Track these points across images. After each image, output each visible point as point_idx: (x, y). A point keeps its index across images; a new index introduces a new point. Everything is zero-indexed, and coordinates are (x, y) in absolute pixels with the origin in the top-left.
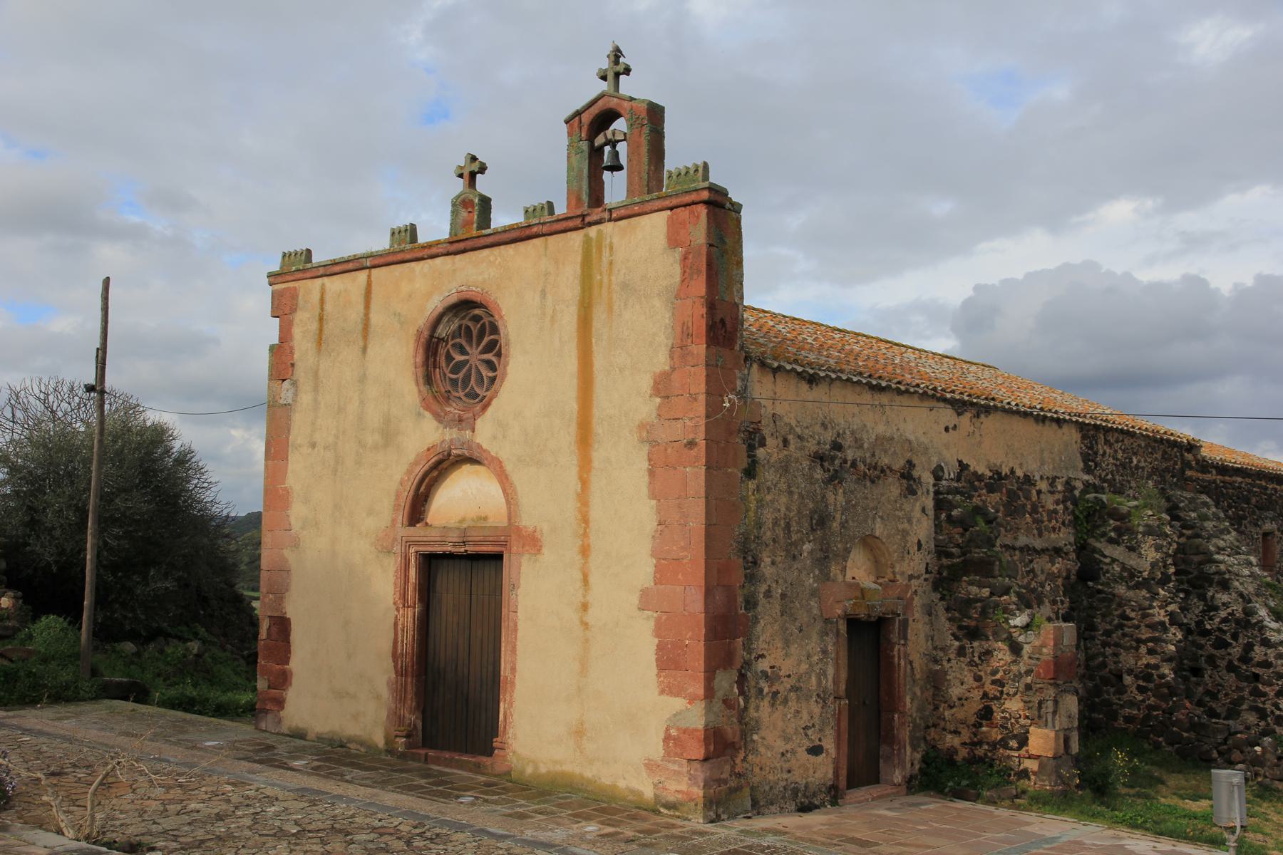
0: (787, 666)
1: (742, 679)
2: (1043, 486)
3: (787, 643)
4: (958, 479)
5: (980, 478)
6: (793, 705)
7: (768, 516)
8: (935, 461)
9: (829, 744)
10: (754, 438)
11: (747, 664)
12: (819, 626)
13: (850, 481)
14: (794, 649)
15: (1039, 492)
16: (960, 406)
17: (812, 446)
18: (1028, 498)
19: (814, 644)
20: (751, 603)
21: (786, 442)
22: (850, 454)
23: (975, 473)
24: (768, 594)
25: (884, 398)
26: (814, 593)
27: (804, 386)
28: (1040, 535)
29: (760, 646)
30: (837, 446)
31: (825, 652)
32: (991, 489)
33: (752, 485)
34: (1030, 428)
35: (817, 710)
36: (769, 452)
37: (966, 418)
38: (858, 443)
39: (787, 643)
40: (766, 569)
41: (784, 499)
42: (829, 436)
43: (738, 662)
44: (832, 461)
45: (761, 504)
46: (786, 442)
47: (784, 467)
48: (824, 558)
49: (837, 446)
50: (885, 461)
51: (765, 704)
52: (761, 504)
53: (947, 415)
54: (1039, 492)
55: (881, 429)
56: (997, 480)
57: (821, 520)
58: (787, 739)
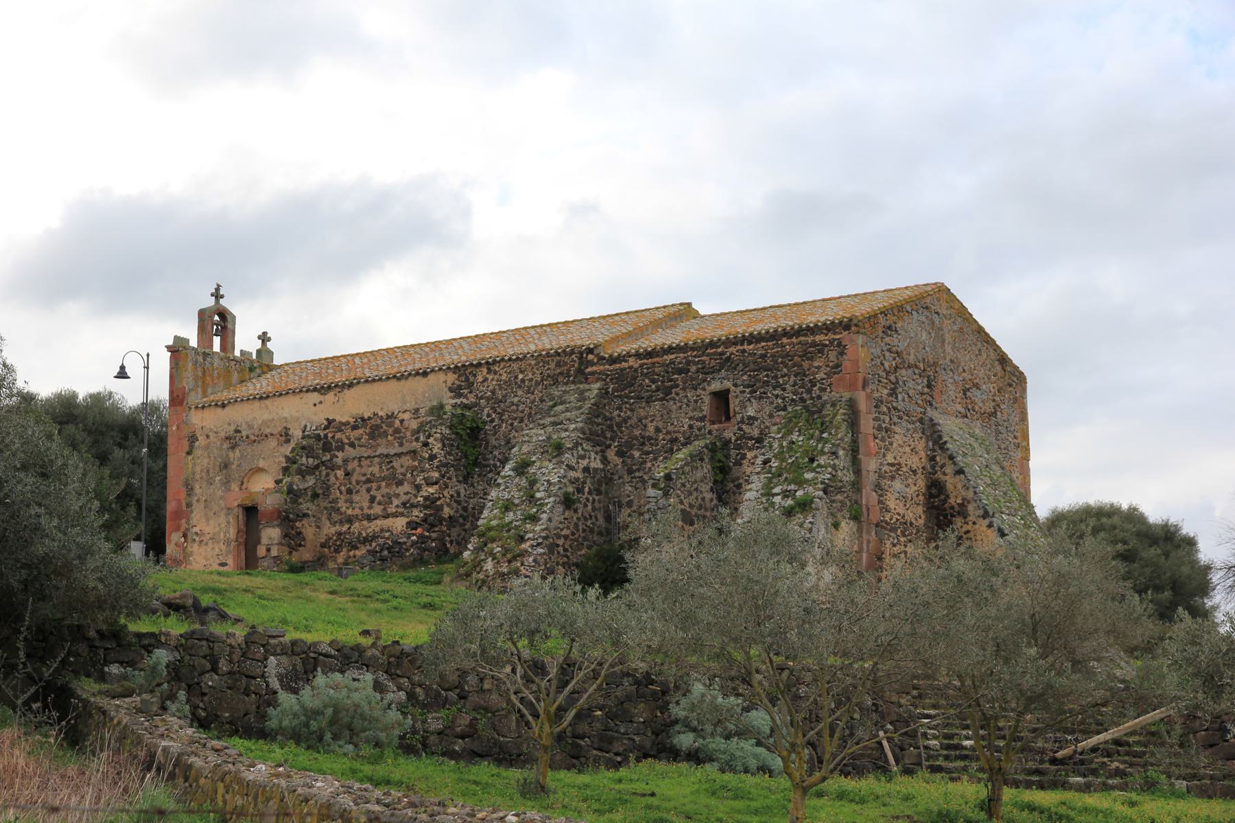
0: (207, 530)
1: (185, 536)
2: (406, 416)
3: (208, 520)
4: (326, 428)
5: (347, 423)
6: (210, 546)
7: (198, 469)
8: (303, 423)
9: (230, 561)
10: (193, 439)
11: (187, 529)
12: (225, 511)
13: (243, 446)
14: (211, 522)
15: (402, 421)
16: (323, 390)
17: (223, 435)
18: (390, 425)
19: (222, 519)
20: (189, 505)
21: (208, 436)
22: (244, 433)
23: (341, 423)
24: (198, 501)
25: (268, 402)
26: (221, 498)
27: (219, 410)
28: (401, 445)
29: (194, 521)
30: (237, 431)
31: (228, 522)
32: (355, 428)
33: (190, 457)
34: (393, 383)
35: (223, 548)
36: (202, 441)
37: (330, 396)
38: (250, 427)
39: (208, 520)
40: (197, 490)
41: (206, 460)
42: (233, 428)
43: (183, 529)
44: (234, 440)
45: (194, 465)
46: (208, 436)
47: (207, 447)
48: (227, 483)
49: (237, 431)
50: (268, 431)
51: (196, 546)
52: (194, 465)
53: (315, 397)
54: (402, 421)
55: (266, 417)
56: (360, 422)
57: (226, 466)
58: (207, 559)
